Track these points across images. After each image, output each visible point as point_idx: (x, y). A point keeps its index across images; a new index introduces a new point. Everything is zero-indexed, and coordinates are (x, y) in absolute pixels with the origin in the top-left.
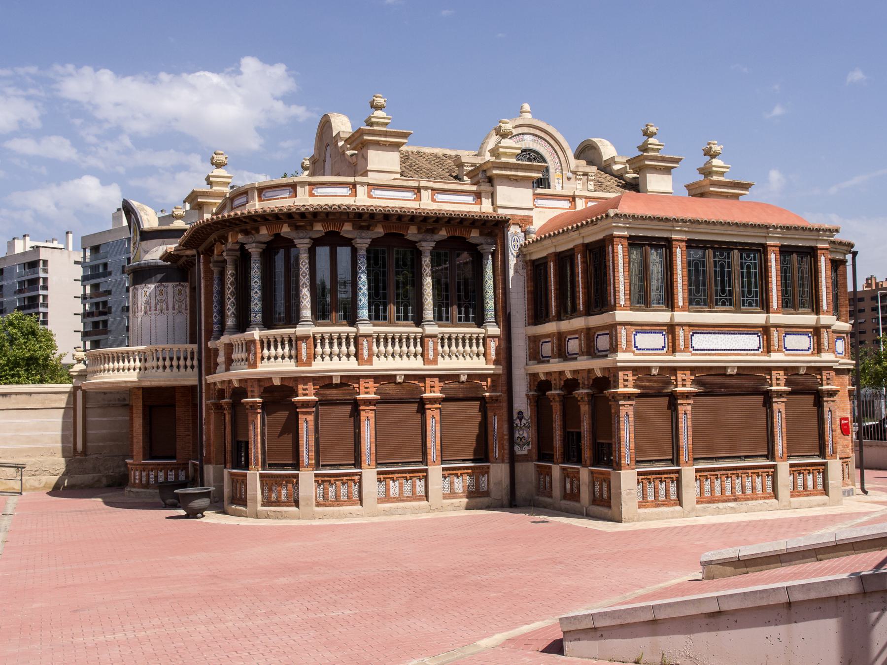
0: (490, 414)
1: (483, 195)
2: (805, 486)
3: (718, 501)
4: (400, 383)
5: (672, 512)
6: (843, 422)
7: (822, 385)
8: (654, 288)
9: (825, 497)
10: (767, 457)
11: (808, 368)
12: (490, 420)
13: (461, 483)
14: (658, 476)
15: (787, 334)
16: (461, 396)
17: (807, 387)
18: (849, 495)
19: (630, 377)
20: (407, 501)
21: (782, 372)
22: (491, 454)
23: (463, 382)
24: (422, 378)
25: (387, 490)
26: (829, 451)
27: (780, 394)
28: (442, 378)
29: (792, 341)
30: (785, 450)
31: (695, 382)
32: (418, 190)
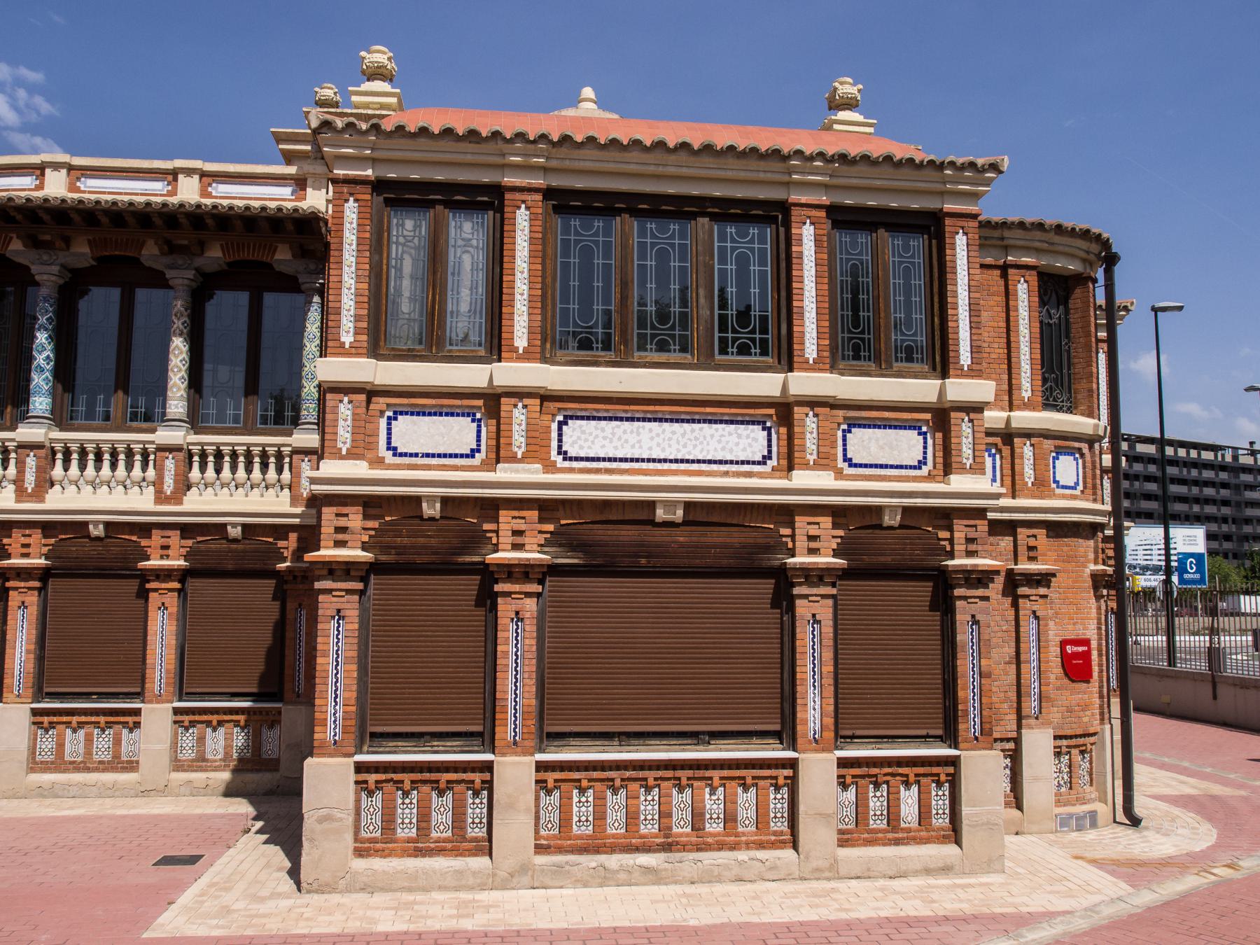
0: (290, 606)
1: (309, 182)
2: (893, 816)
3: (612, 849)
4: (98, 539)
5: (459, 873)
6: (1069, 649)
7: (951, 555)
8: (464, 307)
9: (952, 849)
10: (777, 735)
11: (906, 510)
12: (290, 616)
13: (225, 742)
14: (427, 776)
15: (853, 424)
16: (230, 566)
17: (903, 560)
18: (1079, 829)
19: (355, 520)
20: (96, 770)
21: (826, 521)
22: (287, 686)
23: (235, 541)
24: (145, 530)
25: (61, 746)
26: (970, 725)
27: (815, 576)
28: (186, 530)
29: (868, 444)
30: (830, 721)
31: (555, 540)
32: (174, 174)
